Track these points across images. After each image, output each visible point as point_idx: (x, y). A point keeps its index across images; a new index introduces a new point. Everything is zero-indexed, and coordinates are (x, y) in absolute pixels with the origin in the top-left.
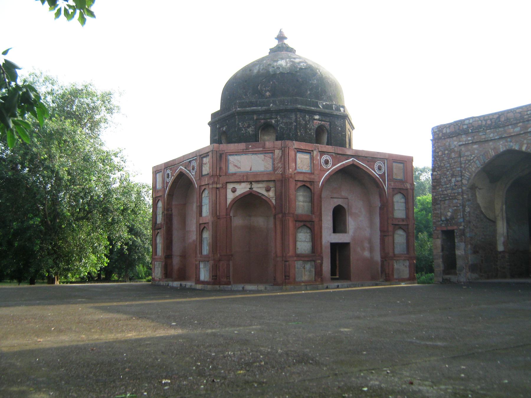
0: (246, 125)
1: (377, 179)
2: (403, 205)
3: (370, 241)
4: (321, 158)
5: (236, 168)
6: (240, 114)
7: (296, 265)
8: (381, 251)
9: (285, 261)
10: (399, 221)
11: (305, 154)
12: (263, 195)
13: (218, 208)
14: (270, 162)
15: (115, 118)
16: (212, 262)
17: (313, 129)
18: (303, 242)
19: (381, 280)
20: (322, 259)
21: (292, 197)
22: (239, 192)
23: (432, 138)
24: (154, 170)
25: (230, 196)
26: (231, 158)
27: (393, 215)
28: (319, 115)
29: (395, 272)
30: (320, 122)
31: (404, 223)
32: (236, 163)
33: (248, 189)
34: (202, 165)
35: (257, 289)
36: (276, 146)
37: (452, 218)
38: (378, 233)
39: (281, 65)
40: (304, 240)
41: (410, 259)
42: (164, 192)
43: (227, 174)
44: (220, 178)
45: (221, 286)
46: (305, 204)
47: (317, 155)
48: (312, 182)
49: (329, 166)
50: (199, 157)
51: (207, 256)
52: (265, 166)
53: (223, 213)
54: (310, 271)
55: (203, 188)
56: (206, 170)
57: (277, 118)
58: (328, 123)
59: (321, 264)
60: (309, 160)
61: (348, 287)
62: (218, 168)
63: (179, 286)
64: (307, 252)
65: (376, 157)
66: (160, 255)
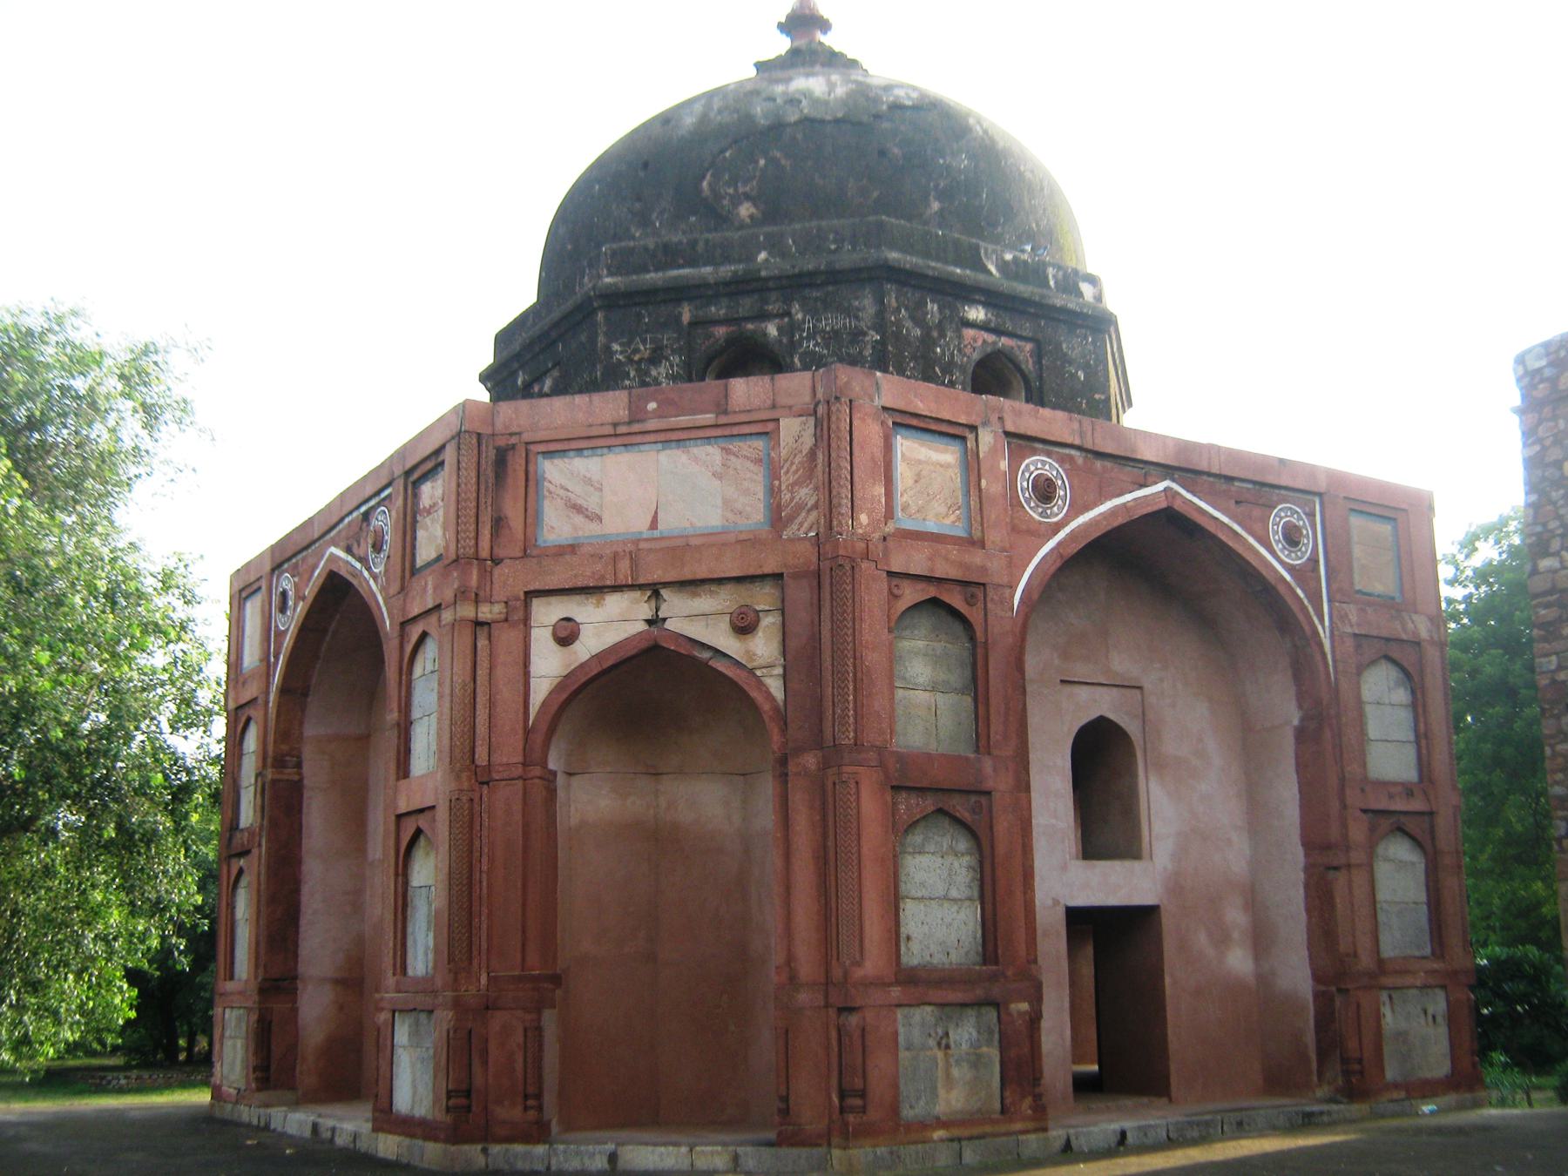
0: (645, 350)
1: (1282, 589)
2: (1405, 716)
3: (1253, 902)
4: (1013, 468)
5: (579, 519)
6: (612, 300)
7: (901, 1030)
8: (1310, 946)
9: (841, 1010)
10: (1391, 797)
11: (940, 443)
12: (717, 652)
13: (482, 730)
15: (171, 442)
16: (445, 1017)
17: (963, 368)
18: (936, 908)
19: (1319, 1093)
20: (1037, 998)
21: (872, 658)
22: (590, 644)
23: (1516, 399)
24: (236, 588)
25: (549, 665)
26: (554, 471)
27: (1364, 765)
28: (986, 305)
29: (1387, 1050)
30: (991, 338)
31: (1417, 805)
32: (578, 492)
33: (642, 627)
34: (415, 522)
35: (684, 1164)
36: (783, 400)
38: (1296, 854)
39: (807, 94)
40: (940, 890)
41: (1446, 981)
42: (268, 675)
43: (528, 550)
44: (496, 571)
45: (496, 1149)
46: (944, 701)
47: (994, 450)
48: (973, 587)
49: (1058, 510)
50: (400, 483)
51: (425, 986)
52: (727, 503)
53: (509, 753)
54: (977, 1062)
55: (415, 632)
56: (432, 540)
57: (788, 314)
58: (1028, 347)
59: (1035, 1019)
60: (955, 477)
61: (1170, 1143)
62: (486, 519)
63: (307, 1133)
64: (956, 957)
65: (1271, 479)
66: (244, 976)
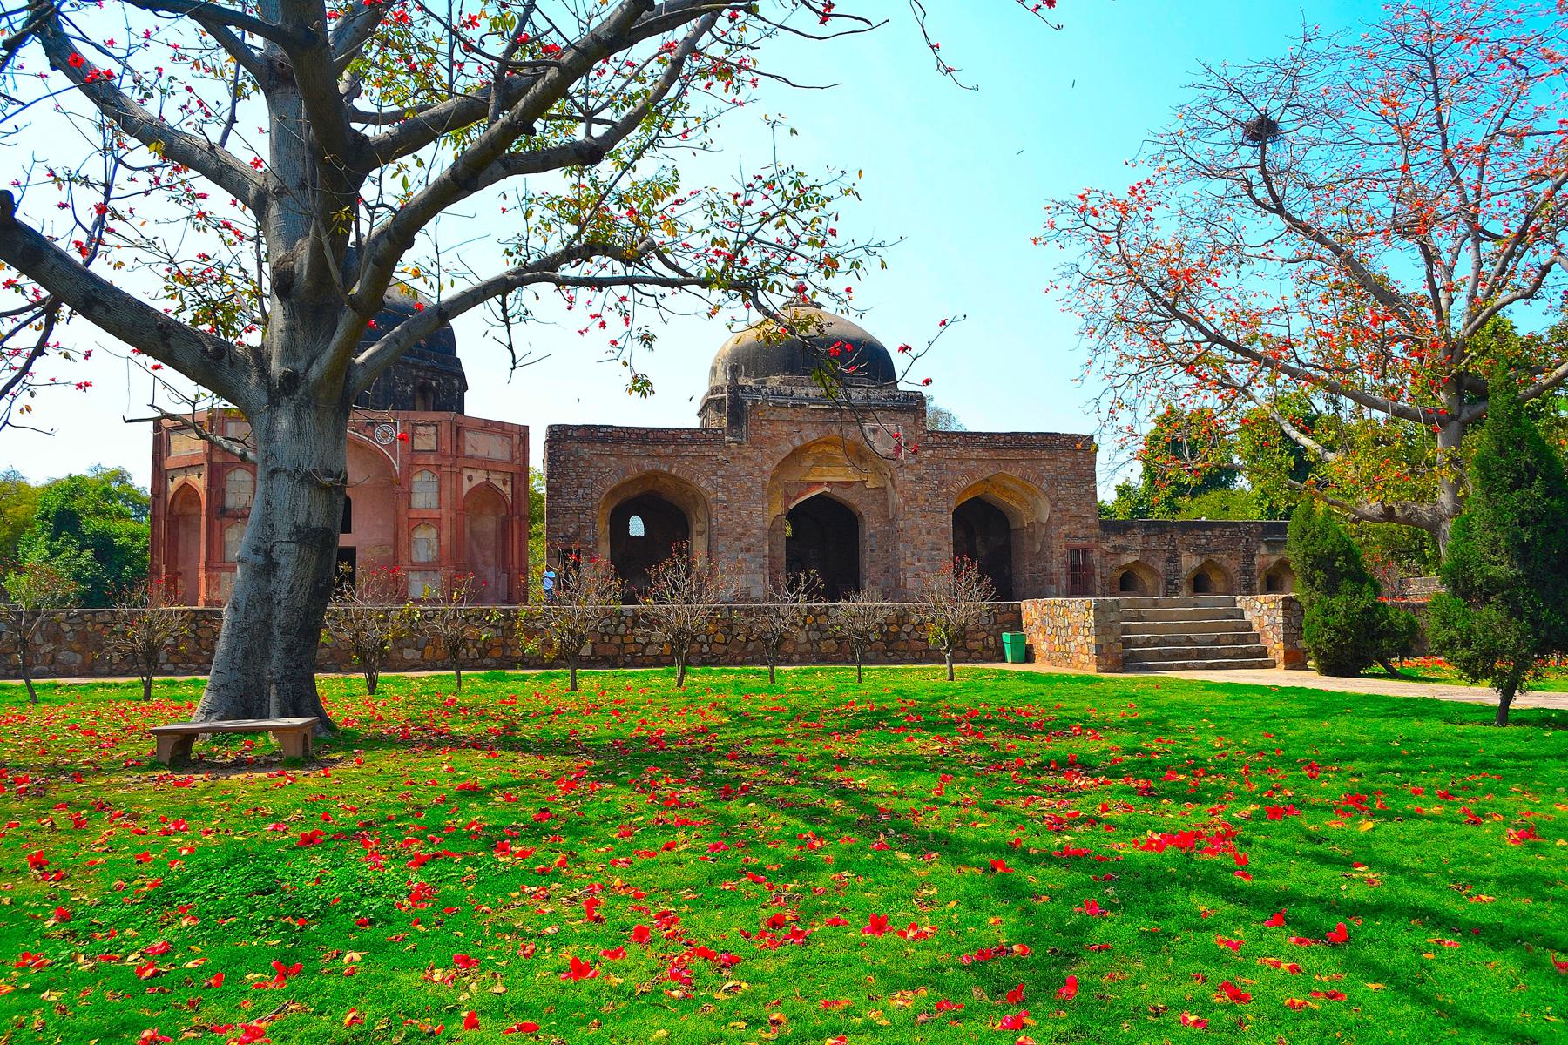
14: (508, 448)
22: (476, 482)
25: (467, 486)
26: (469, 435)
37: (576, 535)
